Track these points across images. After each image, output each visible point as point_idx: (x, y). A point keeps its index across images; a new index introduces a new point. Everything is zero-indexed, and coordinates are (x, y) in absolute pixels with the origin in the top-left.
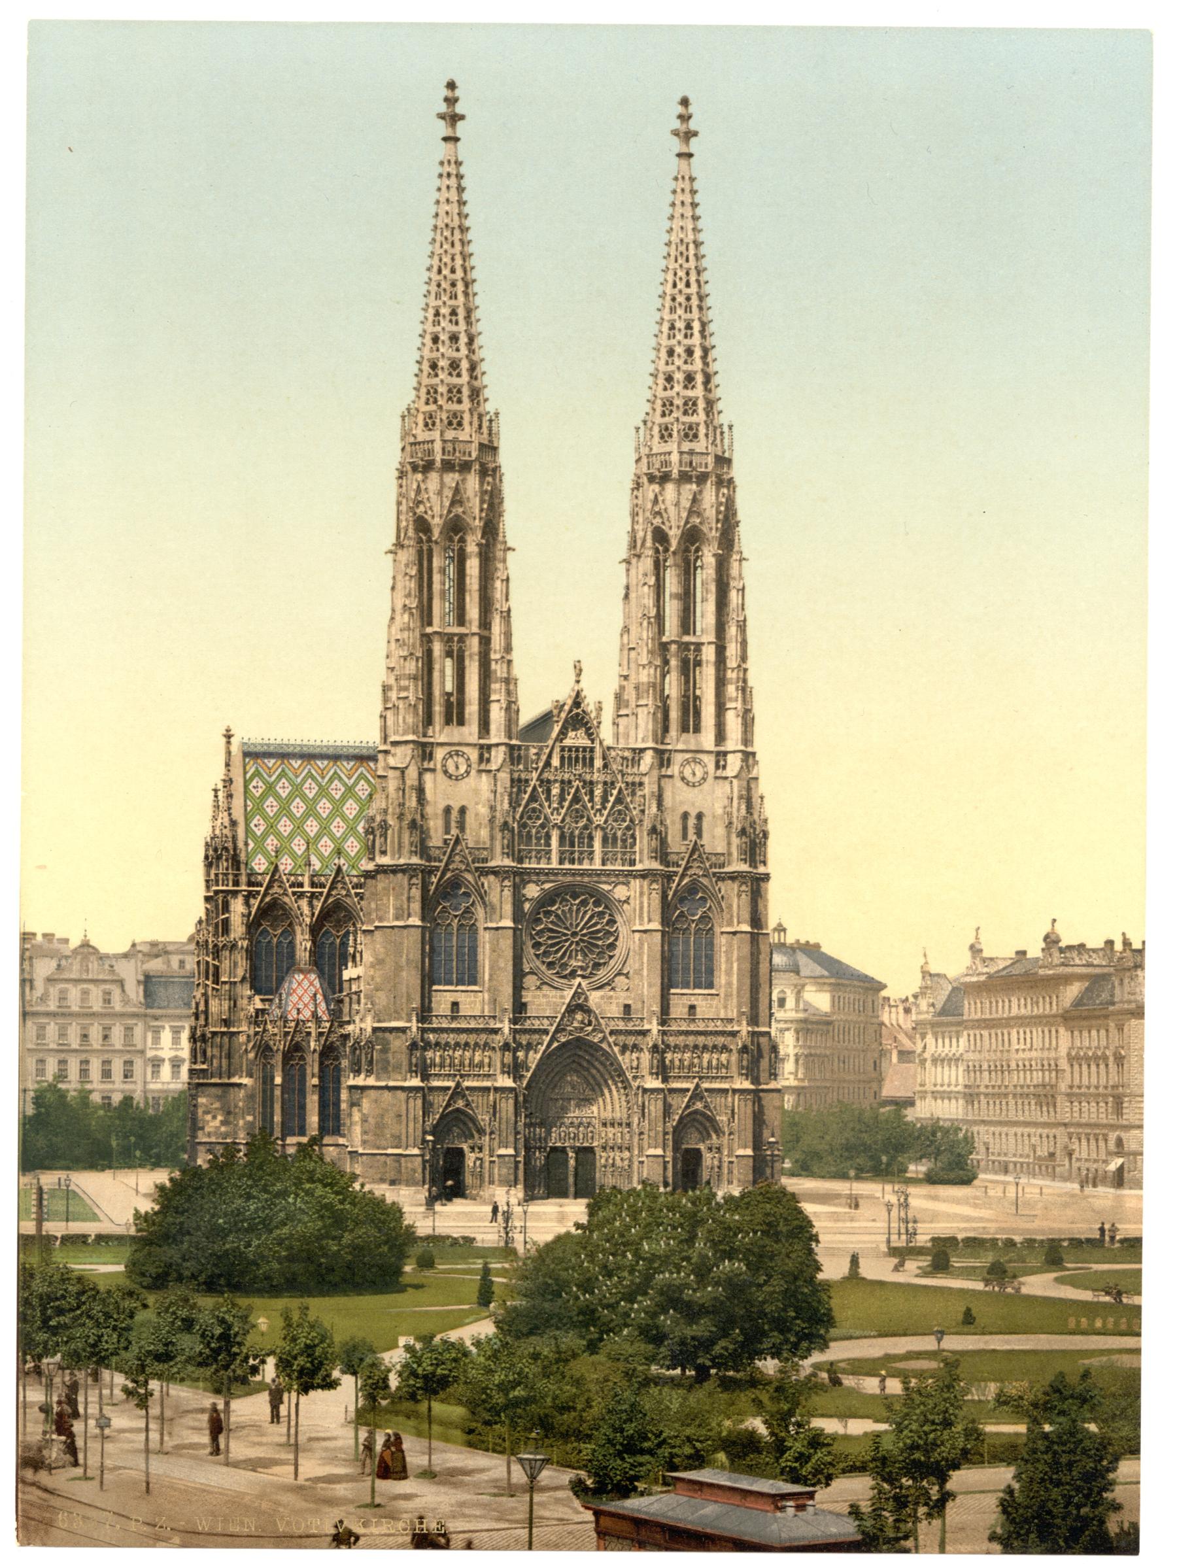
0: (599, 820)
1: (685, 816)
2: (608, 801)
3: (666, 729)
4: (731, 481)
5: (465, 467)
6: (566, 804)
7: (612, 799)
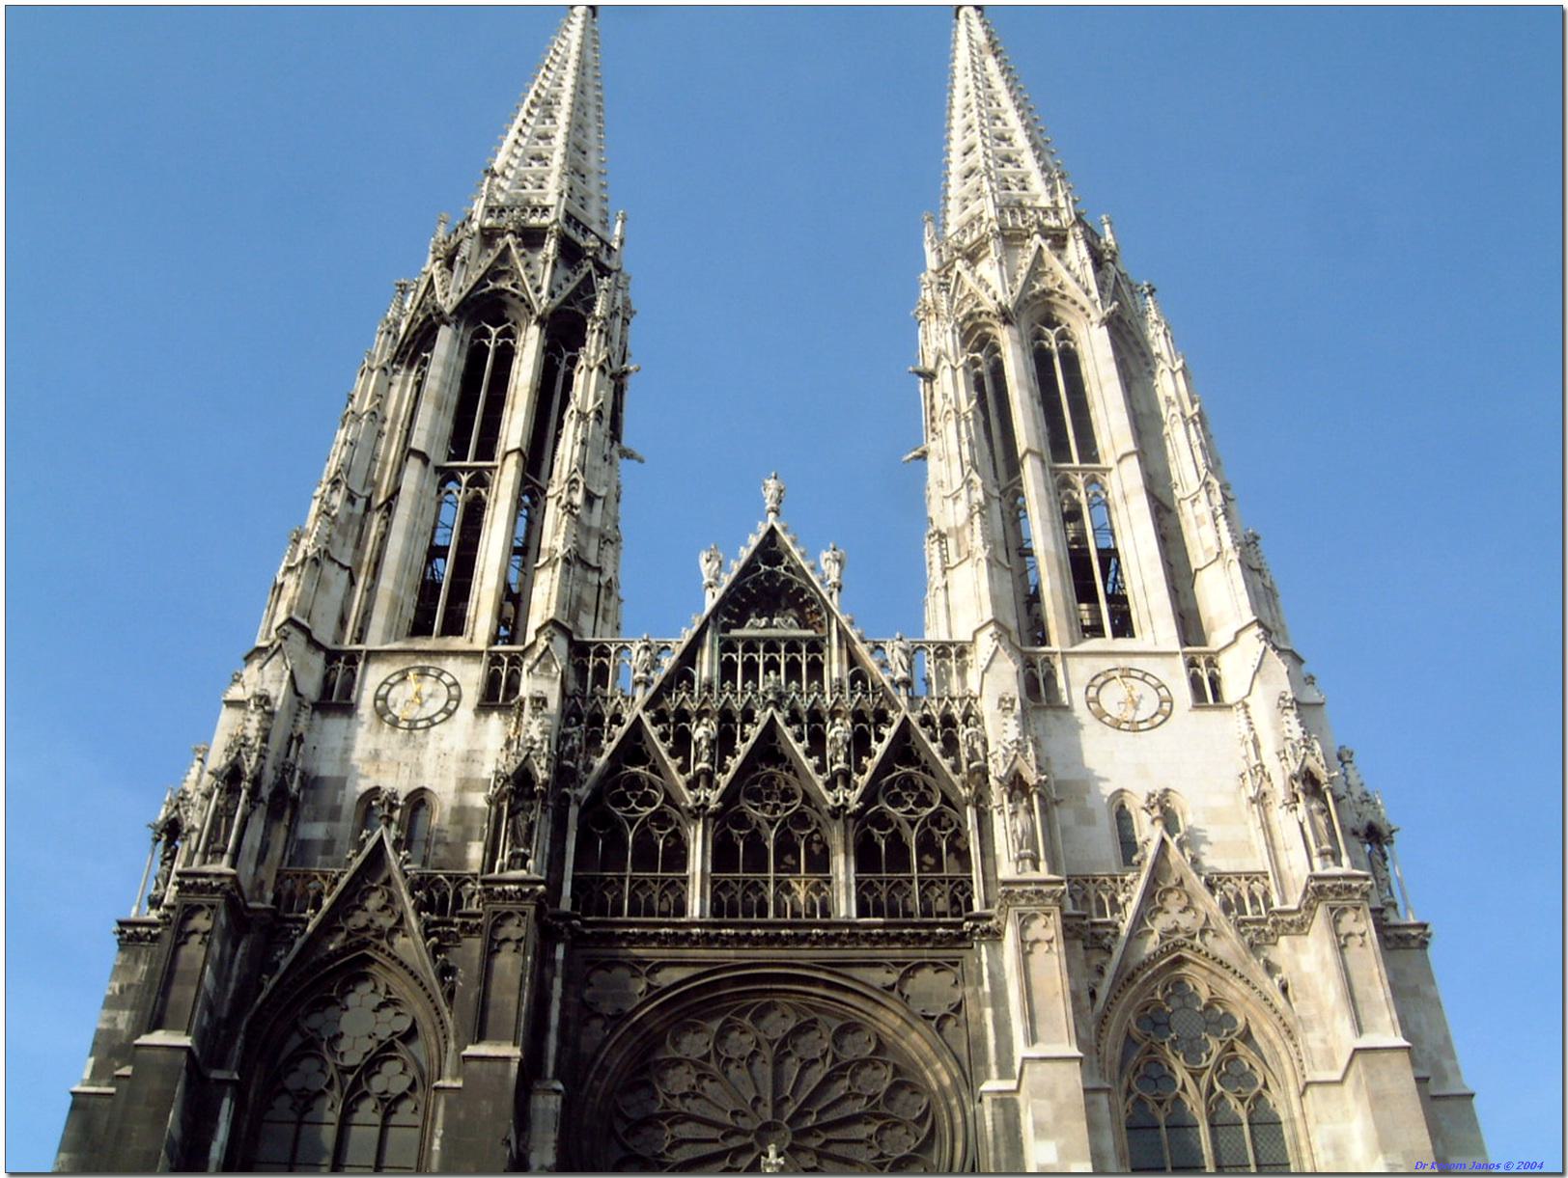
2: (870, 754)
7: (879, 749)
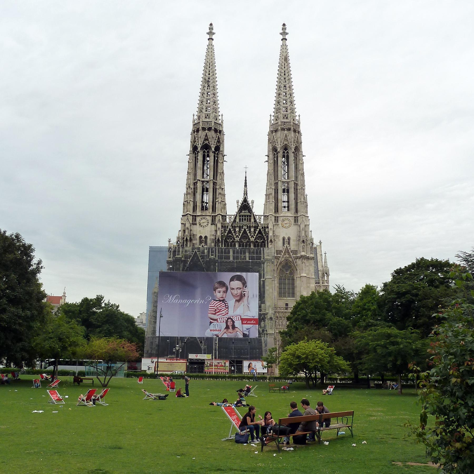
0: (252, 239)
1: (284, 239)
3: (277, 211)
4: (299, 132)
5: (210, 129)
6: (241, 234)
7: (257, 232)
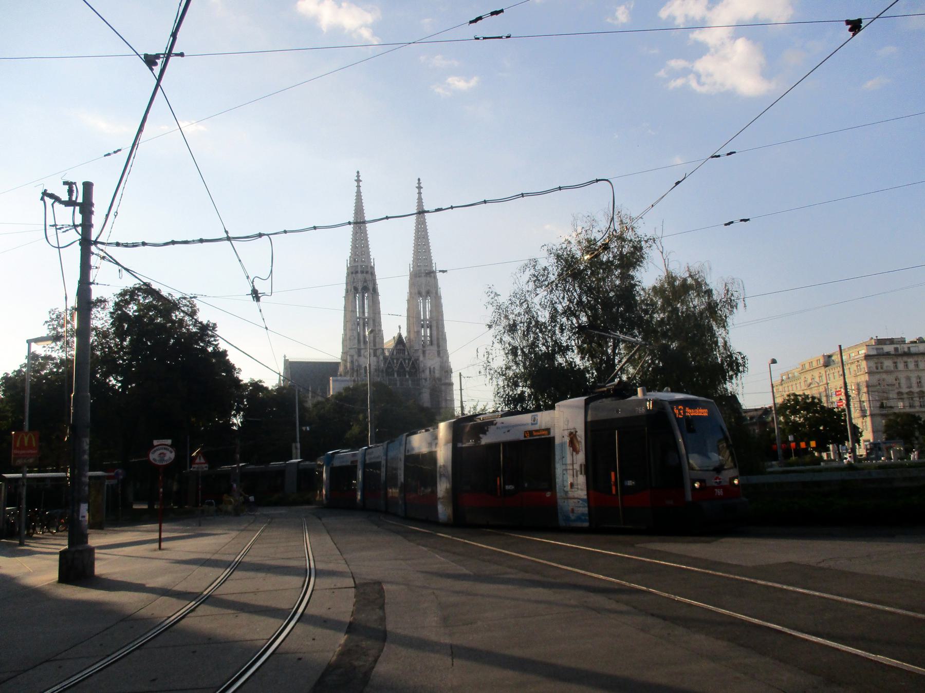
0: (407, 369)
5: (367, 272)
